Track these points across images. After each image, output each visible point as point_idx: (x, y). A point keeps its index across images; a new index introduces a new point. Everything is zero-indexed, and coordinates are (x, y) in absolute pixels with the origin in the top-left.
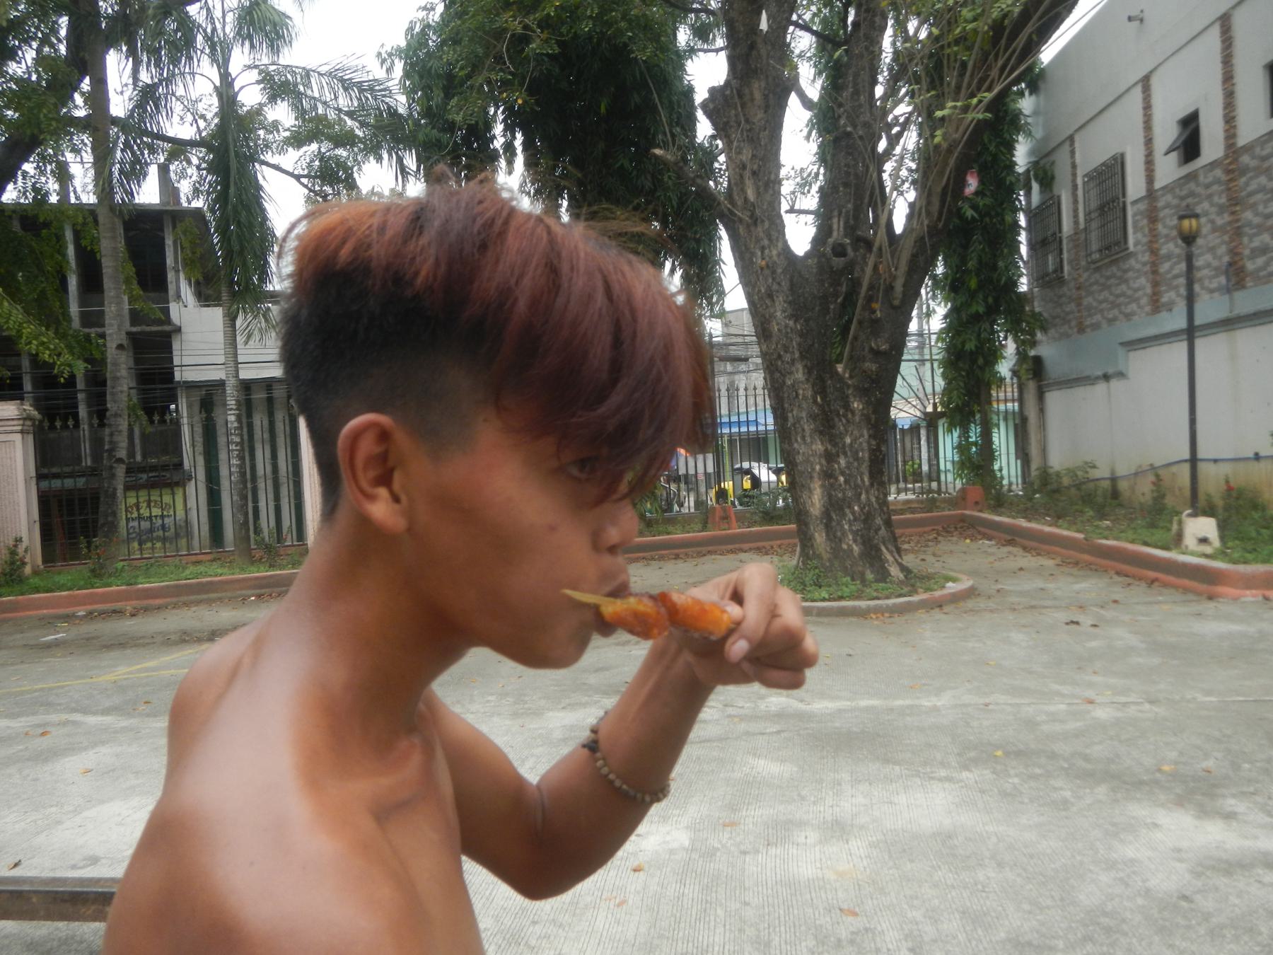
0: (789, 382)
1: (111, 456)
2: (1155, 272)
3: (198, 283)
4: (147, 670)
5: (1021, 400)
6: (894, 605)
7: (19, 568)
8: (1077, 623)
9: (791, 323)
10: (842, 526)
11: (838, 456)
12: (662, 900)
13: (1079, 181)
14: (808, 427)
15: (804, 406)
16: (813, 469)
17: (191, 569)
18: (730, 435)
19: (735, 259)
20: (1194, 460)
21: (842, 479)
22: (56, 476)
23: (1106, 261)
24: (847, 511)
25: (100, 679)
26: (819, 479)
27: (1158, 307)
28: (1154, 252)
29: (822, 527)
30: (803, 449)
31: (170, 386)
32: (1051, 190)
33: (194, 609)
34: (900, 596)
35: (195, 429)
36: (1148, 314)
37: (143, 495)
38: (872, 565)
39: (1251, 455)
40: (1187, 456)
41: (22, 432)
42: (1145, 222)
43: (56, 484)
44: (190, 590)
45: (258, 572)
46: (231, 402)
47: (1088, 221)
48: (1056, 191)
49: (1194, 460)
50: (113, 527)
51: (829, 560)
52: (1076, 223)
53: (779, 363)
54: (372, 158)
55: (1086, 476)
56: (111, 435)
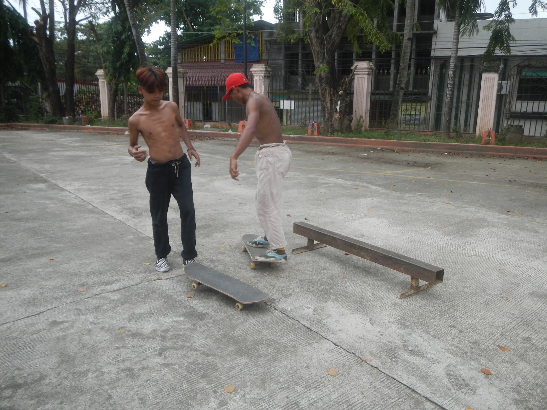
1: (399, 86)
3: (448, 10)
22: (378, 94)
31: (429, 58)
33: (421, 154)
37: (409, 104)
41: (368, 74)
43: (377, 97)
44: (421, 145)
45: (451, 142)
46: (452, 65)
50: (396, 116)
56: (400, 77)
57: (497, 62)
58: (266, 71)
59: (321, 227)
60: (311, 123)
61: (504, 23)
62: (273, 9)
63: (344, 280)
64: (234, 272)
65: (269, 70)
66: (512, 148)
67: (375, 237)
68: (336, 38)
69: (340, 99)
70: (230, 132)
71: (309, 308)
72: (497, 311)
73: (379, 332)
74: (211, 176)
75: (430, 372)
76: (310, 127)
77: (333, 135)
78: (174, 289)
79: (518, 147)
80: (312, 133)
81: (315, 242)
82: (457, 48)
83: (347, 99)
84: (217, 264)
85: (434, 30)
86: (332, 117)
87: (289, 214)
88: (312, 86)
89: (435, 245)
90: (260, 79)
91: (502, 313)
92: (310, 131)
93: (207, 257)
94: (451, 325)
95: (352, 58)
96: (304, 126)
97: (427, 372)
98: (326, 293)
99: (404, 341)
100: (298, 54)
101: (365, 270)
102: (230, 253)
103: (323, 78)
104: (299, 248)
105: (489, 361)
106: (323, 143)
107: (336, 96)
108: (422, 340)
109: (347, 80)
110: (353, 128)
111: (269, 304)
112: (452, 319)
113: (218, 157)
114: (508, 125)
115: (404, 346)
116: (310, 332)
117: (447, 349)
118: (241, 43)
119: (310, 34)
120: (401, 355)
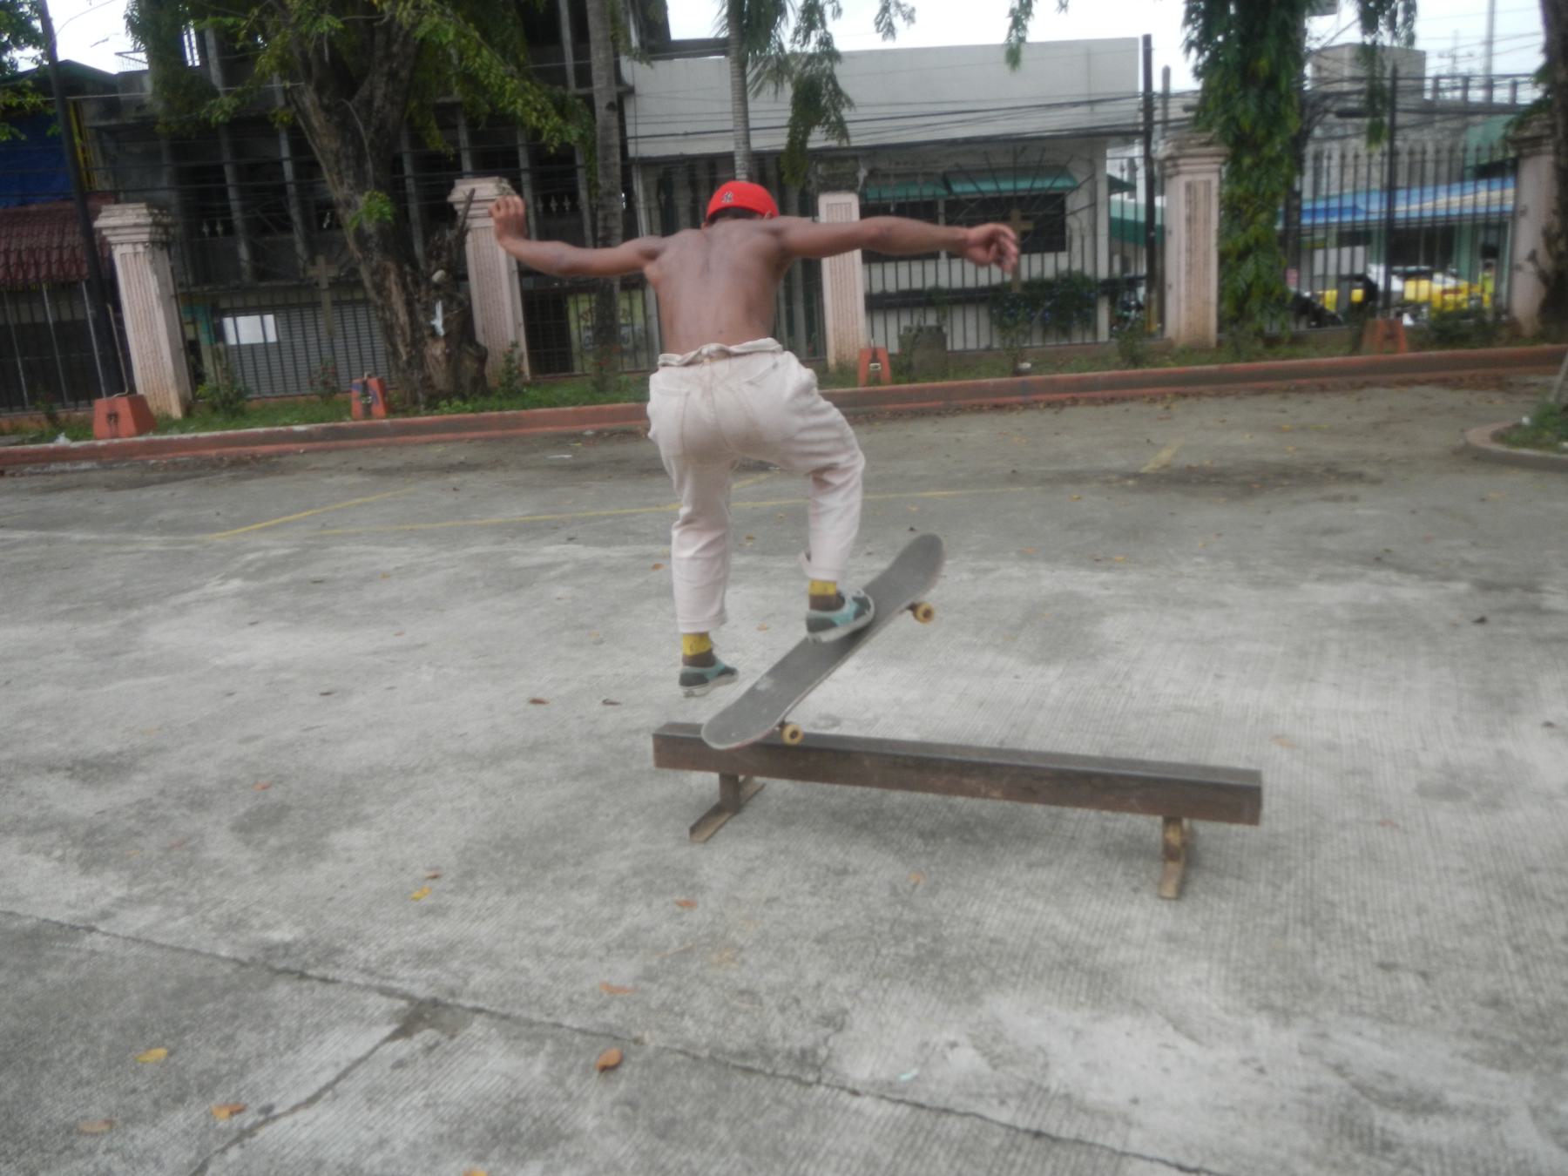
7: (516, 377)
18: (1340, 223)
56: (605, 219)
57: (851, 162)
58: (155, 224)
59: (680, 719)
60: (357, 381)
61: (821, 61)
62: (124, 22)
64: (555, 977)
65: (166, 220)
67: (869, 715)
68: (388, 107)
69: (441, 298)
70: (62, 441)
71: (953, 1045)
73: (1245, 1062)
74: (113, 608)
75: (1525, 1161)
76: (356, 393)
77: (436, 407)
78: (382, 1143)
79: (946, 383)
80: (368, 411)
81: (741, 778)
82: (748, 130)
83: (461, 296)
84: (456, 965)
86: (422, 357)
87: (539, 696)
88: (328, 262)
90: (136, 254)
92: (357, 406)
93: (392, 945)
95: (402, 170)
96: (329, 390)
97: (1518, 1164)
99: (1339, 1069)
100: (219, 170)
101: (967, 842)
102: (462, 900)
103: (370, 236)
106: (412, 438)
107: (423, 287)
109: (450, 235)
110: (492, 382)
111: (811, 1077)
112: (1357, 938)
113: (78, 536)
115: (1356, 1086)
116: (1057, 1149)
118: (23, 137)
119: (296, 96)
120: (1389, 1126)
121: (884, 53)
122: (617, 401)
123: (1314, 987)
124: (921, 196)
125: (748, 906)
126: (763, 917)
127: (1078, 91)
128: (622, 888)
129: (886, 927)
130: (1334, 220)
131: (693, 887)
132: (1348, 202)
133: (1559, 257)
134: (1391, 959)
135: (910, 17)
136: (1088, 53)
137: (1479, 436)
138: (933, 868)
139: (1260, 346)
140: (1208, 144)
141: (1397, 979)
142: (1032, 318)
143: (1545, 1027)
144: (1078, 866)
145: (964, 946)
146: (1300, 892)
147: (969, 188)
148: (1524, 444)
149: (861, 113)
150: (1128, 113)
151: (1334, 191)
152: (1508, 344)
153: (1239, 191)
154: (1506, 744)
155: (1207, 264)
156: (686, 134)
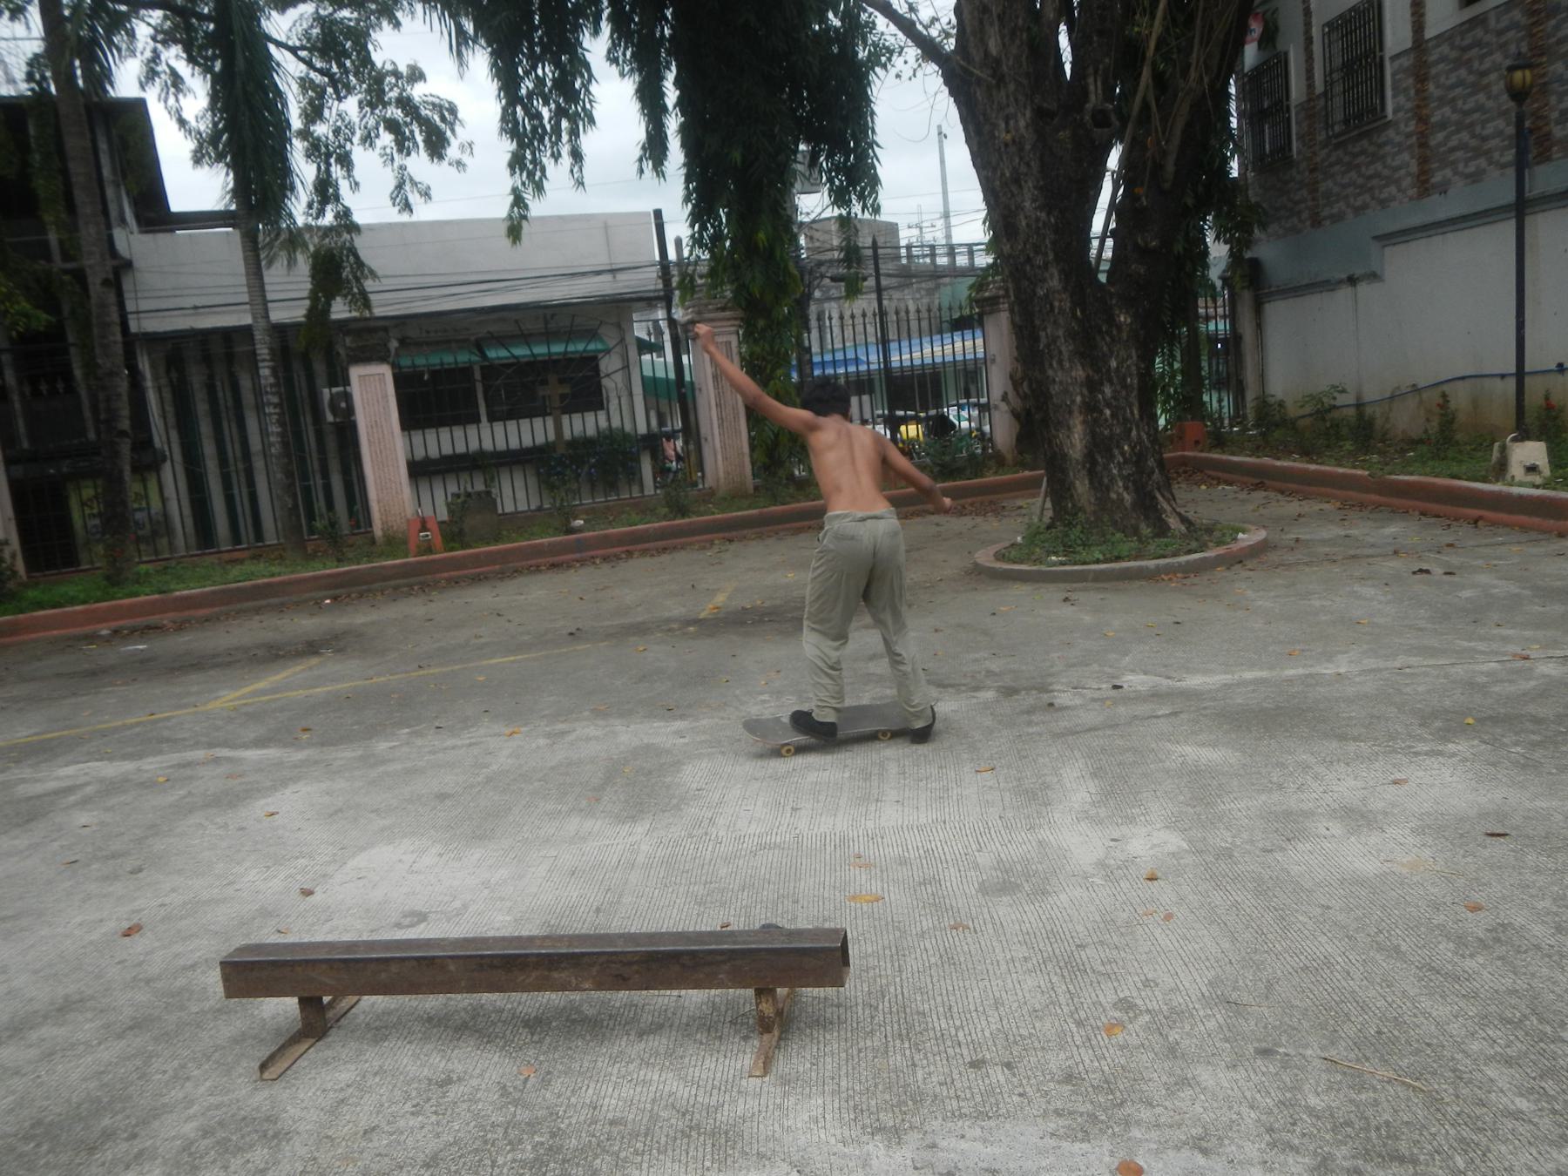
0: (1041, 293)
2: (1423, 145)
4: (263, 692)
5: (1233, 316)
6: (1188, 562)
7: (9, 579)
8: (1427, 572)
9: (1043, 215)
10: (1110, 471)
11: (1102, 384)
12: (1219, 912)
13: (1316, 32)
14: (1066, 349)
15: (1061, 321)
16: (1073, 402)
17: (235, 571)
19: (965, 129)
20: (1520, 374)
21: (1108, 412)
23: (1356, 133)
24: (1116, 452)
25: (210, 706)
26: (1081, 413)
27: (1427, 189)
28: (1423, 121)
29: (1084, 472)
30: (1060, 376)
32: (1275, 47)
33: (257, 617)
34: (1190, 552)
35: (164, 395)
36: (1411, 199)
38: (1147, 518)
39: (1553, 366)
40: (1513, 370)
42: (1411, 81)
45: (325, 568)
46: (263, 351)
47: (1329, 84)
48: (1280, 47)
49: (1520, 374)
51: (1095, 512)
52: (1310, 86)
53: (1028, 268)
54: (385, 24)
55: (1332, 402)
61: (339, 235)
63: (557, 1085)
66: (490, 553)
67: (457, 904)
72: (990, 967)
79: (501, 547)
82: (265, 302)
85: (122, 258)
89: (641, 859)
91: (1003, 967)
94: (968, 1059)
98: (564, 1161)
104: (279, 1049)
105: (1151, 1105)
108: (979, 1146)
112: (949, 1043)
114: (458, 496)
117: (1052, 1134)
121: (404, 225)
122: (136, 595)
123: (918, 1099)
124: (456, 362)
125: (344, 1143)
126: (361, 1153)
127: (601, 261)
128: (190, 1154)
129: (500, 1131)
130: (841, 371)
131: (275, 1136)
132: (851, 355)
133: (1024, 397)
134: (980, 1056)
135: (426, 194)
136: (606, 225)
137: (984, 557)
138: (542, 1058)
139: (792, 490)
140: (723, 309)
141: (988, 1076)
142: (579, 475)
143: (1112, 1093)
144: (687, 1025)
145: (584, 1135)
146: (894, 1010)
147: (503, 353)
148: (1021, 562)
149: (387, 283)
150: (649, 280)
151: (838, 345)
152: (996, 473)
153: (758, 349)
154: (1044, 834)
155: (736, 418)
156: (196, 308)
